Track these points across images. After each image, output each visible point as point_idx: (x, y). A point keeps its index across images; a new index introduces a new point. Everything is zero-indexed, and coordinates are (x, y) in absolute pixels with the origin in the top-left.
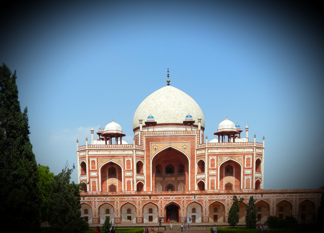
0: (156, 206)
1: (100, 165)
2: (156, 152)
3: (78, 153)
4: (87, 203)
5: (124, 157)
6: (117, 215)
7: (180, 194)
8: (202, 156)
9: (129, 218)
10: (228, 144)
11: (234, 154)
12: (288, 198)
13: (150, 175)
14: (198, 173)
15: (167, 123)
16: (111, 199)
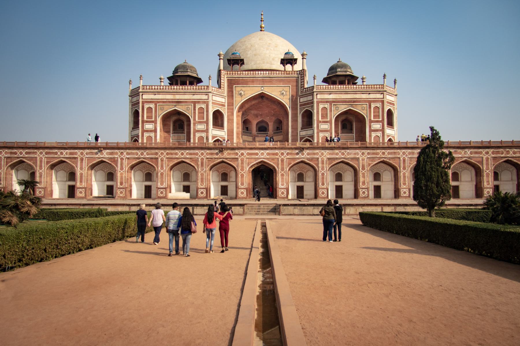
0: (233, 169)
1: (160, 113)
2: (243, 98)
3: (131, 98)
4: (107, 161)
5: (195, 103)
6: (162, 184)
7: (277, 147)
8: (308, 104)
9: (186, 189)
10: (346, 88)
11: (354, 102)
12: (472, 156)
13: (233, 130)
14: (302, 129)
15: (260, 68)
16: (152, 154)
